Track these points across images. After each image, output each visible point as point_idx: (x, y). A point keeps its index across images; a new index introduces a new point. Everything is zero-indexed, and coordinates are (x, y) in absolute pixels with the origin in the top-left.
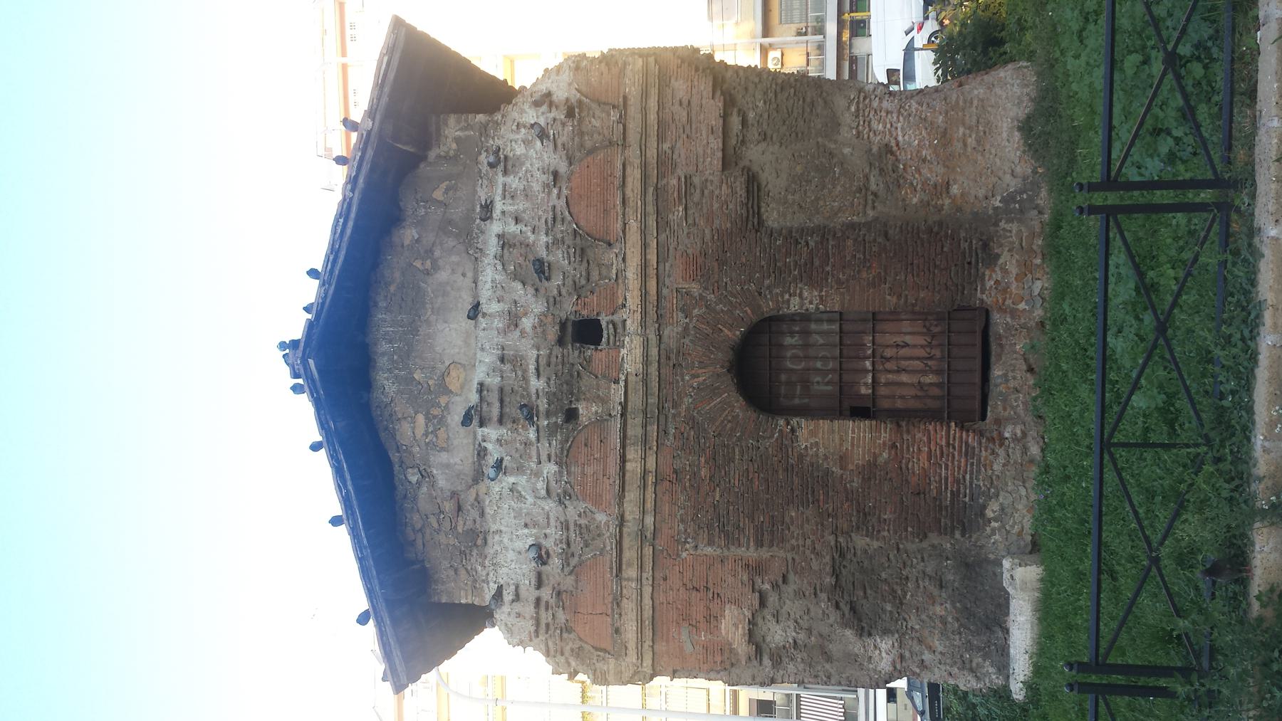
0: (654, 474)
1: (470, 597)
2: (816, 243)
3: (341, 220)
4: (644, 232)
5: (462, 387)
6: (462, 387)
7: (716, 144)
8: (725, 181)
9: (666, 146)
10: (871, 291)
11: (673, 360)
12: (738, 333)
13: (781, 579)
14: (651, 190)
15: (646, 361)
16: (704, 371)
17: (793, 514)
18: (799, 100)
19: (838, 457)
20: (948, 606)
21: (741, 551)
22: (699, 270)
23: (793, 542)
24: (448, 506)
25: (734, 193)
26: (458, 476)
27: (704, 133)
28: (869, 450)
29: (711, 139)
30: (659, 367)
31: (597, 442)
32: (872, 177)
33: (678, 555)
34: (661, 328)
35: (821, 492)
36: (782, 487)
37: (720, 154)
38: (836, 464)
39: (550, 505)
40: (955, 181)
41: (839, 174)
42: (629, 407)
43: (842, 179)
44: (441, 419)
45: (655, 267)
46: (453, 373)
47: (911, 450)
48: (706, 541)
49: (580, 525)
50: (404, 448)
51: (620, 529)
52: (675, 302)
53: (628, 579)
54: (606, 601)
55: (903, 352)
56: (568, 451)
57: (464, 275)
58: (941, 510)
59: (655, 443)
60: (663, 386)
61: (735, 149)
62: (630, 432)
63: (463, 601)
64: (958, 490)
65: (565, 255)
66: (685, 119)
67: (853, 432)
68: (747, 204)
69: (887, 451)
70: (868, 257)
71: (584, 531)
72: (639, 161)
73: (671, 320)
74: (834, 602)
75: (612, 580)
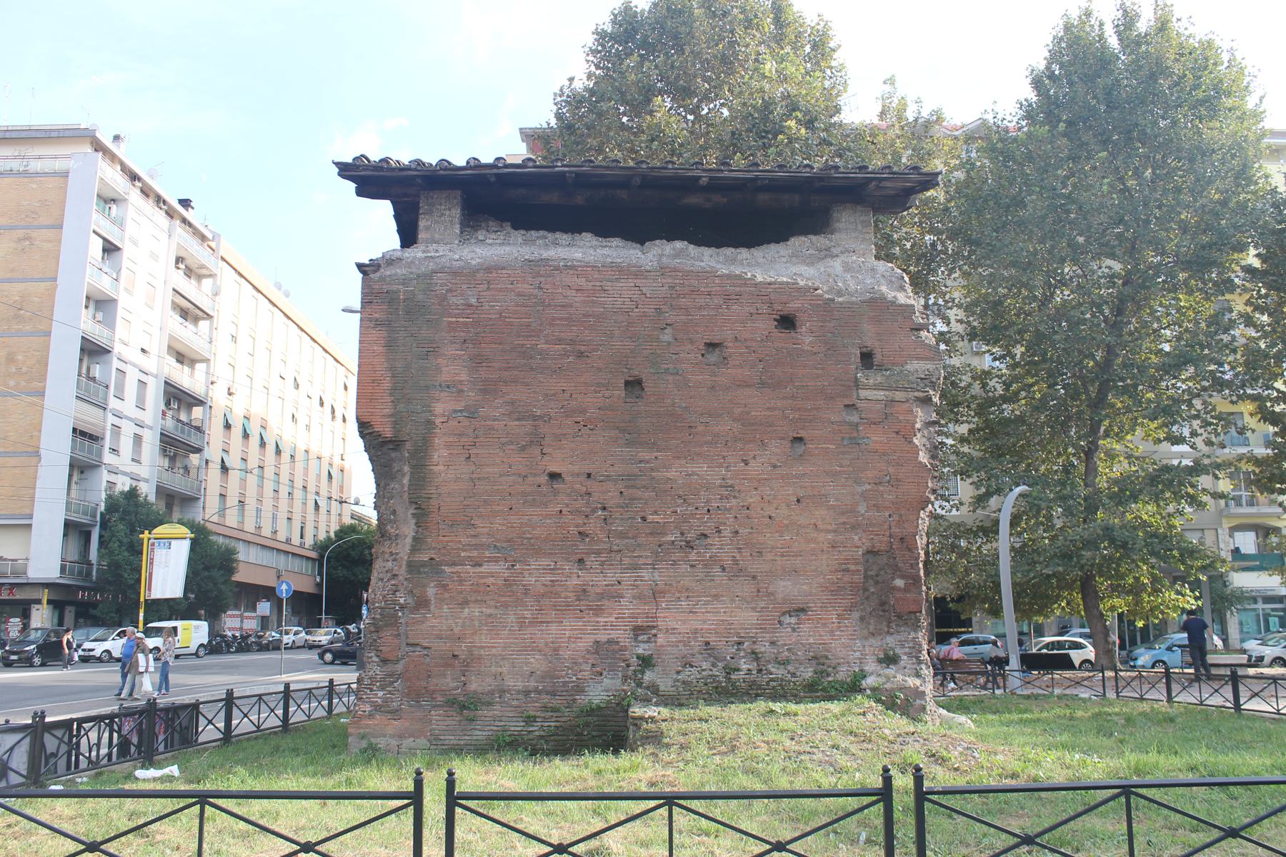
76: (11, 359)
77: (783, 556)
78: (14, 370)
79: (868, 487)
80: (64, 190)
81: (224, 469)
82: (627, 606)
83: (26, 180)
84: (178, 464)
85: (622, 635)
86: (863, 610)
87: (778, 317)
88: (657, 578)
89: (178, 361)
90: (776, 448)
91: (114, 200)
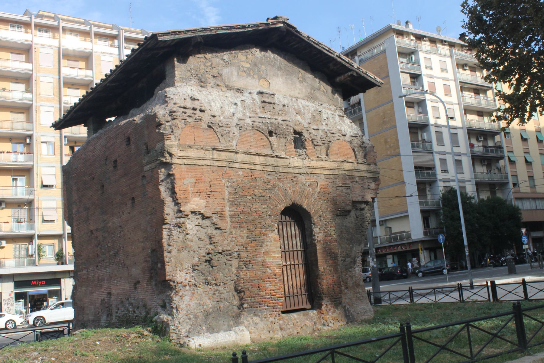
1: (178, 76)
2: (335, 238)
3: (328, 49)
4: (335, 169)
6: (261, 86)
7: (360, 199)
9: (357, 179)
11: (294, 179)
12: (305, 207)
13: (218, 227)
14: (346, 172)
15: (294, 168)
17: (245, 232)
20: (211, 305)
21: (227, 209)
23: (234, 232)
24: (215, 72)
25: (347, 205)
26: (228, 78)
28: (271, 264)
29: (361, 197)
33: (223, 178)
39: (235, 121)
40: (348, 290)
42: (279, 159)
43: (349, 247)
44: (249, 74)
46: (266, 83)
48: (230, 191)
49: (229, 133)
51: (233, 152)
53: (213, 154)
55: (294, 276)
57: (299, 93)
58: (254, 297)
60: (285, 174)
62: (270, 159)
63: (176, 72)
64: (262, 304)
66: (365, 187)
67: (277, 257)
68: (344, 211)
71: (228, 134)
74: (210, 252)
76: (386, 142)
77: (133, 256)
78: (388, 146)
80: (386, 58)
81: (528, 163)
82: (106, 284)
83: (373, 60)
84: (493, 167)
85: (105, 296)
86: (156, 280)
87: (127, 140)
89: (479, 115)
90: (129, 203)
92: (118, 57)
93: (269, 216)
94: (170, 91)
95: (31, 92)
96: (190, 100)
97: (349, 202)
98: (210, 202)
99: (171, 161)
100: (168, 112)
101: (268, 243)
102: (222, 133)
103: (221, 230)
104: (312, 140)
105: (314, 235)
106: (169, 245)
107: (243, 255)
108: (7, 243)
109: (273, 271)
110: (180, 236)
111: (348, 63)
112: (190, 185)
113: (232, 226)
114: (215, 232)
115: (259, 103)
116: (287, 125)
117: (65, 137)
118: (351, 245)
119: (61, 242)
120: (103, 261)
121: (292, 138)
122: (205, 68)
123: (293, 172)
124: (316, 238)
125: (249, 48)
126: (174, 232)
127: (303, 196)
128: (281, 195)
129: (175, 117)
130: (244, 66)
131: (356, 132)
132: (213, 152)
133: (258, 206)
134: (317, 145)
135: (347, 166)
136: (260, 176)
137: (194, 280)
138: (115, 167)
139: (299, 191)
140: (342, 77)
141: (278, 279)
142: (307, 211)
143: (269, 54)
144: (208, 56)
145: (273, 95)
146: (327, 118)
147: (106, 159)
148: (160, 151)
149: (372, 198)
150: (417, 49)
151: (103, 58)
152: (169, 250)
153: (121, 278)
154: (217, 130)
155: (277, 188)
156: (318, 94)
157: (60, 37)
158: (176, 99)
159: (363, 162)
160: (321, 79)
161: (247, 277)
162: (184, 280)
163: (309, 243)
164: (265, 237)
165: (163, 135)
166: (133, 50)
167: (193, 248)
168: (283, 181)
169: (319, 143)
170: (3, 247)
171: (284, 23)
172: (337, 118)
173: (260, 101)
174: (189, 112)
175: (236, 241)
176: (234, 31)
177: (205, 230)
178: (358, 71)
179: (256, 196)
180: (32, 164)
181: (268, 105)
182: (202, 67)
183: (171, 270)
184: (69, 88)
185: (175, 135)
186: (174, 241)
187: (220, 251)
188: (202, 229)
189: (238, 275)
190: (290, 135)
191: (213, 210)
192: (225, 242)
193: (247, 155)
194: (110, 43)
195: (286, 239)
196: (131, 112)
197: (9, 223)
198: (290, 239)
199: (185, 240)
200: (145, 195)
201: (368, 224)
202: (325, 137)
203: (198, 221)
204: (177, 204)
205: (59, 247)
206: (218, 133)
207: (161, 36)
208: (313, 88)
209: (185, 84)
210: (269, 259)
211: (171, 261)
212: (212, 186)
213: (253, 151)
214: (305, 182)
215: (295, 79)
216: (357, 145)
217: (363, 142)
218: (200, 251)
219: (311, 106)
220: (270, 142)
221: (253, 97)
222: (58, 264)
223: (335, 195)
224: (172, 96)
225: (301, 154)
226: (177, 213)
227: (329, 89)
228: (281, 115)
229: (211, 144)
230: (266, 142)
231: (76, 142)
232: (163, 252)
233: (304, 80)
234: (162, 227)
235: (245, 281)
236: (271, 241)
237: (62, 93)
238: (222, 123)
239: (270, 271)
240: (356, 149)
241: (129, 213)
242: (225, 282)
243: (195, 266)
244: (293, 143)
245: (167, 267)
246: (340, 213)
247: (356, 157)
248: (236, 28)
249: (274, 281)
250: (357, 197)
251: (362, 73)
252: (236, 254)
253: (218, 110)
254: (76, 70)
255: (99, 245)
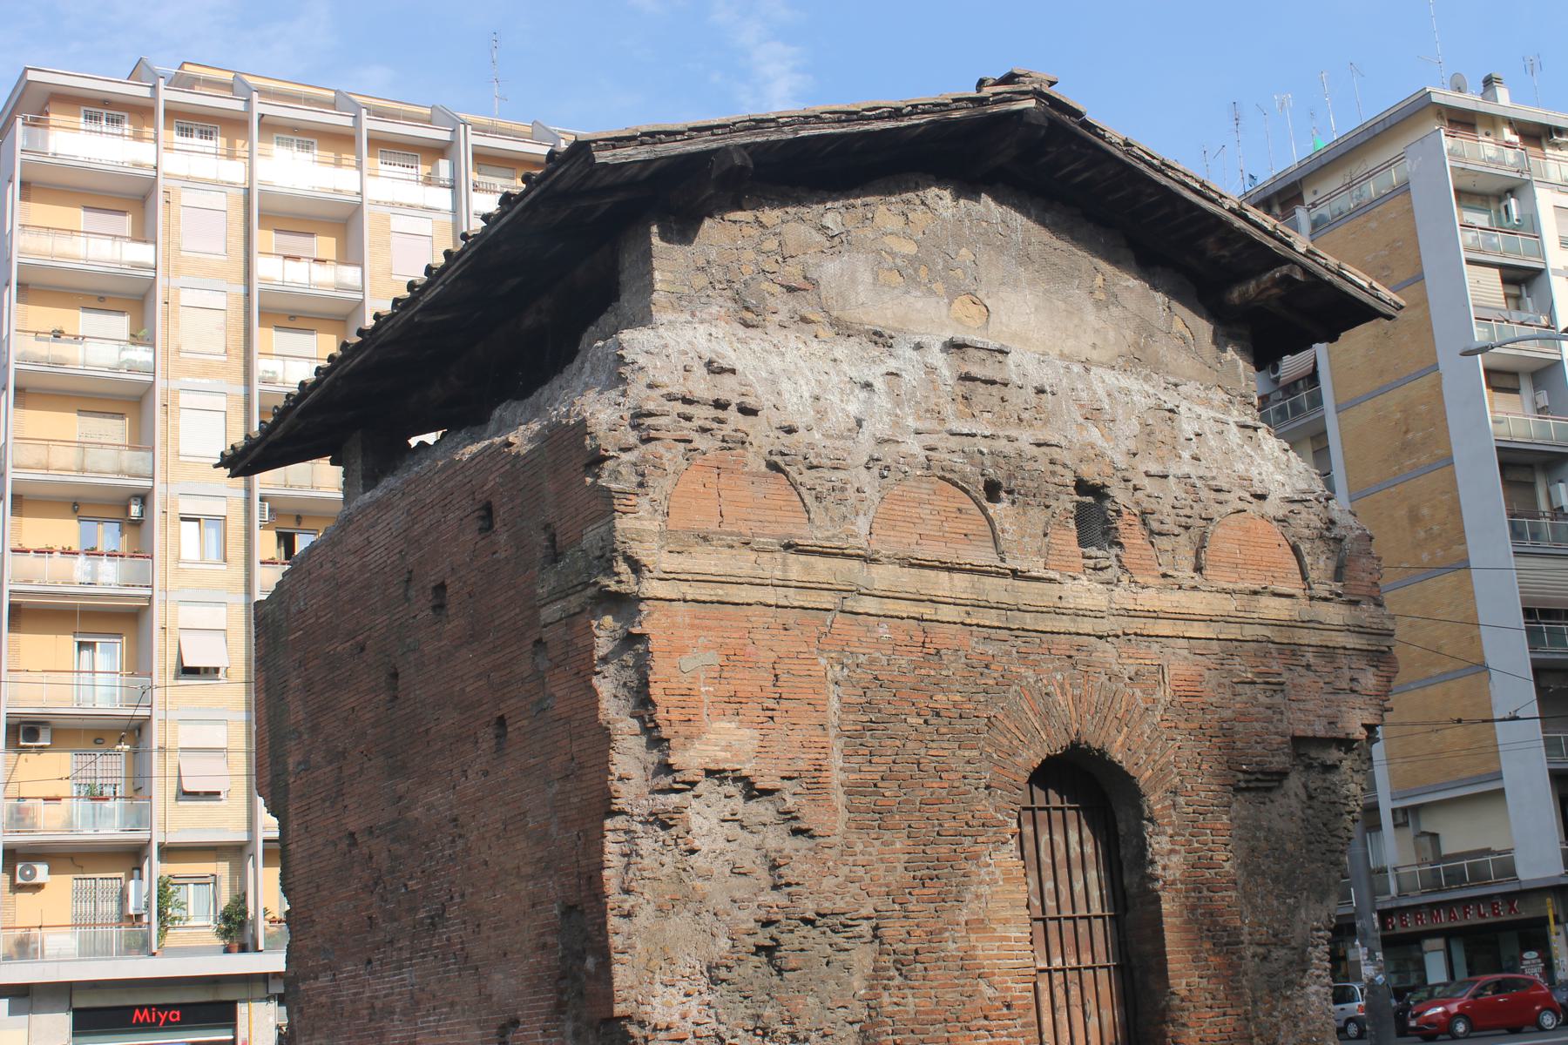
0: (934, 618)
1: (664, 287)
3: (1197, 186)
4: (1226, 620)
5: (958, 320)
6: (958, 320)
7: (1320, 730)
8: (1284, 739)
9: (1310, 657)
10: (1190, 957)
11: (1078, 656)
12: (1119, 757)
13: (804, 826)
14: (1267, 632)
15: (1078, 614)
16: (1071, 703)
17: (898, 846)
18: (1343, 844)
19: (982, 917)
21: (836, 761)
22: (1184, 699)
23: (859, 847)
24: (792, 272)
26: (840, 294)
27: (1328, 711)
29: (1325, 721)
30: (1070, 634)
31: (964, 526)
32: (1285, 951)
34: (1114, 640)
35: (933, 891)
36: (933, 826)
37: (1310, 734)
38: (973, 914)
39: (865, 445)
41: (1289, 905)
45: (1187, 635)
46: (974, 309)
47: (1005, 1032)
48: (846, 699)
49: (843, 490)
50: (870, 216)
51: (859, 556)
52: (1147, 662)
53: (785, 564)
54: (740, 523)
56: (948, 480)
57: (1094, 346)
59: (975, 622)
61: (1303, 755)
63: (657, 275)
65: (1183, 502)
67: (1017, 940)
68: (1262, 772)
69: (997, 994)
70: (1225, 949)
71: (838, 495)
72: (1297, 618)
73: (1124, 655)
74: (774, 917)
75: (773, 536)
76: (1414, 518)
77: (495, 929)
78: (1422, 534)
79: (557, 786)
83: (1362, 219)
86: (577, 1018)
87: (483, 513)
88: (414, 980)
90: (487, 737)
91: (1511, 192)
92: (449, 218)
93: (987, 787)
94: (634, 340)
95: (150, 342)
96: (705, 371)
97: (1279, 739)
98: (773, 735)
99: (636, 588)
100: (627, 415)
101: (984, 889)
102: (819, 489)
103: (812, 837)
104: (1143, 513)
105: (1152, 862)
106: (627, 892)
107: (892, 930)
108: (50, 872)
109: (1002, 990)
110: (667, 859)
111: (1271, 234)
112: (702, 677)
113: (854, 825)
114: (791, 844)
115: (950, 382)
116: (1052, 462)
117: (262, 499)
118: (1291, 901)
119: (239, 873)
120: (391, 942)
121: (1070, 506)
122: (760, 259)
123: (1073, 630)
124: (1159, 871)
125: (916, 188)
126: (646, 845)
127: (1110, 717)
128: (1031, 715)
129: (653, 433)
130: (896, 249)
131: (1304, 486)
132: (784, 559)
133: (946, 753)
134: (1160, 534)
135: (1273, 608)
136: (954, 644)
137: (714, 1020)
138: (439, 607)
139: (1095, 698)
140: (1252, 286)
141: (1019, 1022)
142: (1126, 774)
143: (987, 206)
144: (770, 215)
145: (1001, 352)
146: (1198, 435)
147: (409, 581)
148: (598, 553)
149: (1363, 725)
150: (1526, 177)
151: (398, 223)
152: (627, 906)
153: (452, 1005)
154: (799, 479)
155: (1015, 687)
156: (1164, 349)
157: (251, 151)
158: (657, 369)
159: (1331, 592)
160: (1175, 294)
161: (907, 1012)
162: (676, 1017)
163: (1133, 890)
164: (970, 866)
165: (608, 494)
166: (506, 199)
167: (710, 904)
168: (1036, 664)
169: (1170, 526)
170: (39, 887)
171: (1038, 94)
172: (1234, 436)
173: (955, 376)
174: (702, 414)
175: (867, 880)
176: (862, 128)
177: (757, 839)
178: (1308, 262)
179: (938, 714)
180: (147, 592)
181: (981, 387)
182: (749, 255)
183: (631, 979)
184: (278, 328)
185: (651, 495)
186: (645, 874)
187: (810, 915)
188: (745, 833)
189: (873, 1003)
190: (1063, 497)
191: (785, 767)
192: (828, 883)
193: (906, 570)
194: (423, 169)
195: (1047, 873)
196: (497, 413)
197: (63, 801)
198: (1062, 873)
199: (683, 874)
200: (544, 710)
201: (1354, 821)
202: (1189, 502)
203: (732, 803)
204: (657, 742)
205: (232, 887)
206: (803, 490)
207: (605, 148)
208: (1145, 329)
209: (687, 316)
210: (987, 945)
211: (632, 947)
212: (783, 677)
213: (929, 552)
214: (1116, 668)
215: (1079, 295)
216: (1307, 532)
217: (1332, 522)
218: (735, 912)
219: (1140, 390)
220: (990, 521)
221: (929, 360)
222: (227, 950)
223: (1227, 714)
224: (642, 361)
225: (1103, 563)
226: (655, 775)
227: (1204, 328)
228: (1031, 426)
229: (780, 530)
230: (977, 524)
231: (299, 519)
232: (604, 914)
233: (1112, 298)
234: (602, 826)
235: (899, 1026)
236: (994, 882)
237: (257, 347)
238: (818, 455)
239: (990, 992)
240: (1305, 547)
241: (486, 773)
242: (827, 1030)
243: (717, 967)
244: (1072, 524)
245: (617, 968)
246: (1247, 781)
247: (1304, 578)
248: (869, 118)
249: (1006, 1028)
250: (1310, 724)
251: (1323, 272)
252: (865, 928)
253: (804, 406)
254: (303, 266)
255: (376, 884)
